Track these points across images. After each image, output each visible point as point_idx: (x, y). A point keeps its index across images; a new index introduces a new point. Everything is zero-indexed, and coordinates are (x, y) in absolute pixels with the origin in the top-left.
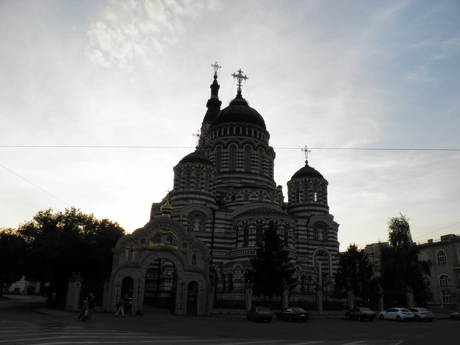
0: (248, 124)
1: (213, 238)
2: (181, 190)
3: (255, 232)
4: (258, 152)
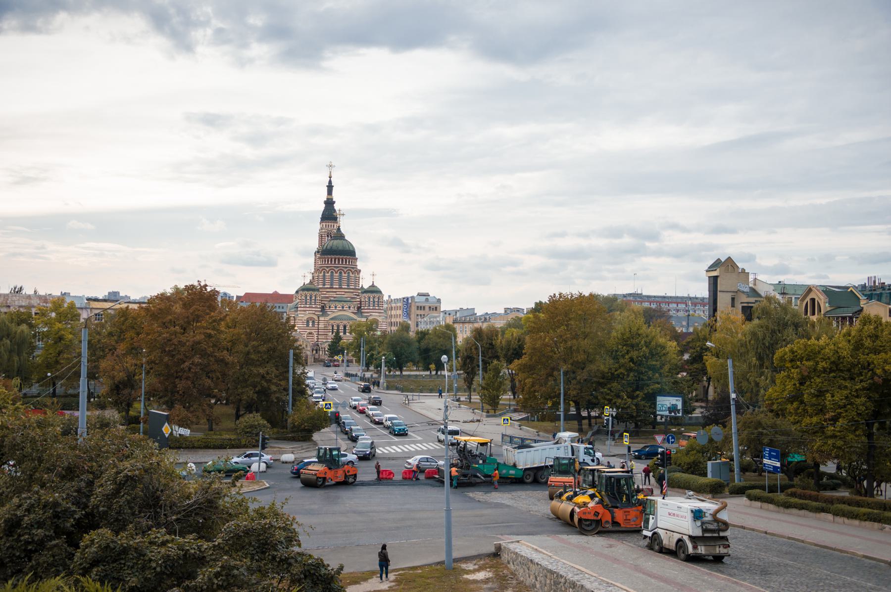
0: (341, 257)
1: (318, 329)
2: (302, 306)
3: (336, 328)
4: (347, 275)
